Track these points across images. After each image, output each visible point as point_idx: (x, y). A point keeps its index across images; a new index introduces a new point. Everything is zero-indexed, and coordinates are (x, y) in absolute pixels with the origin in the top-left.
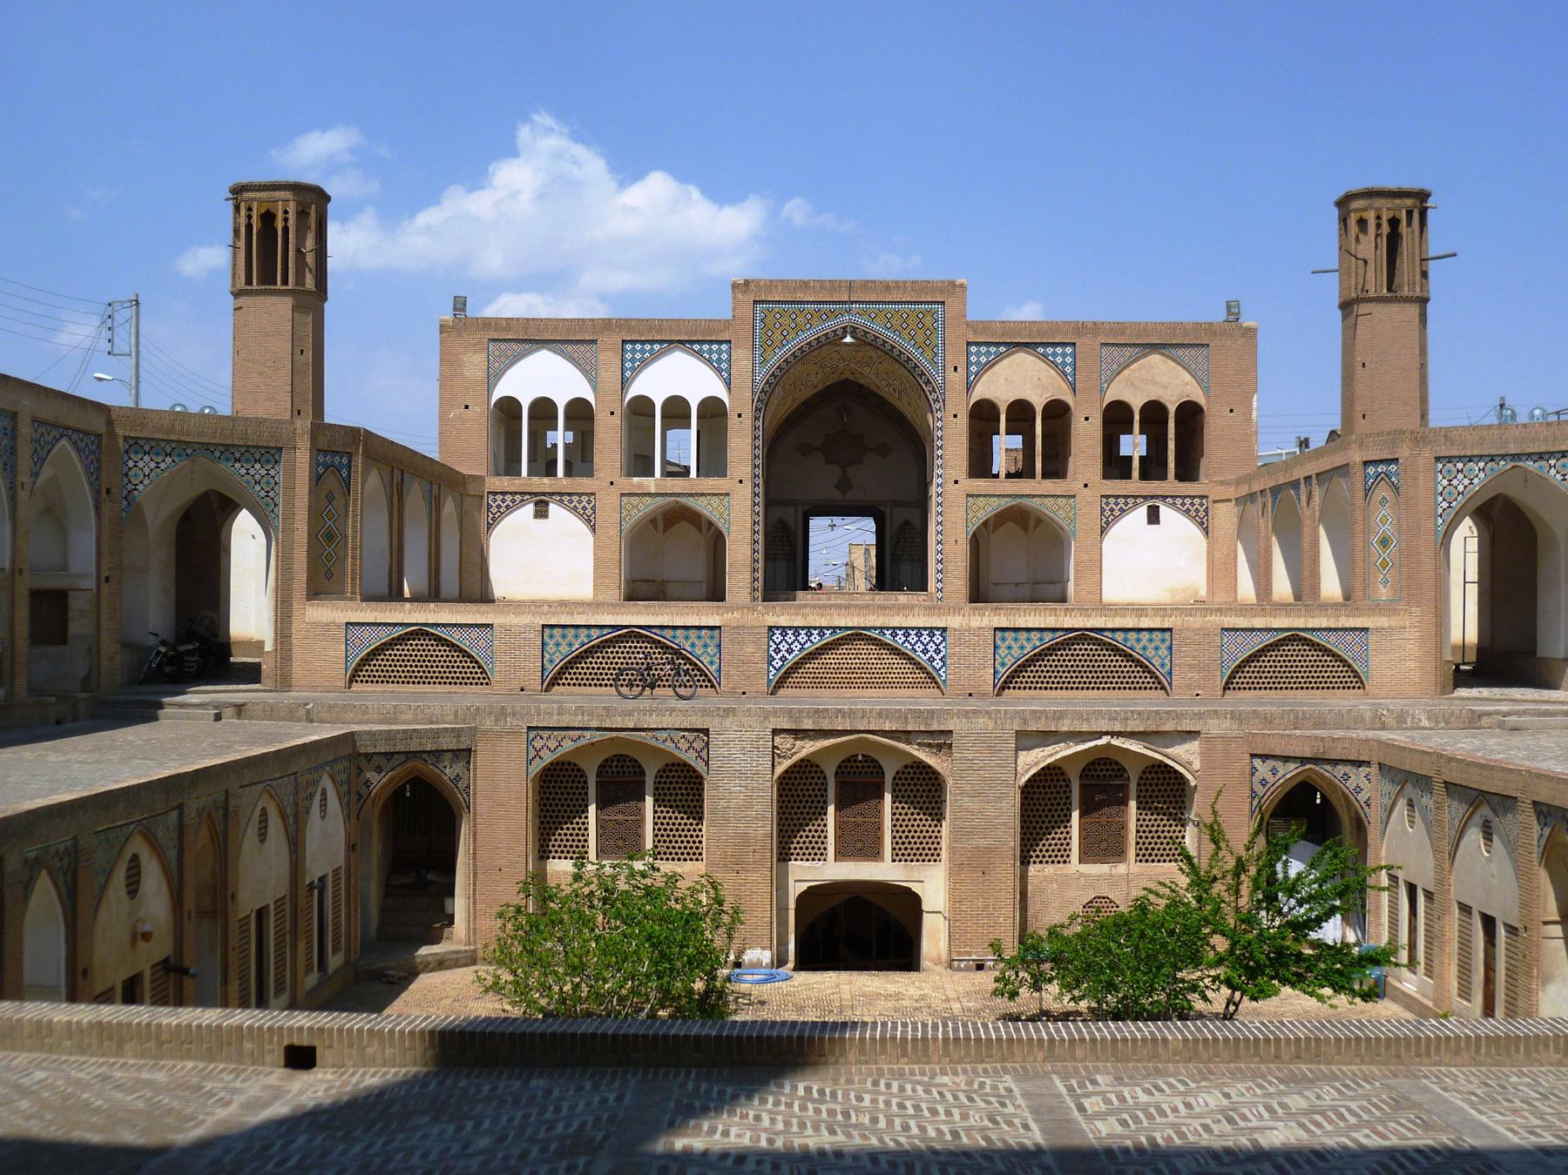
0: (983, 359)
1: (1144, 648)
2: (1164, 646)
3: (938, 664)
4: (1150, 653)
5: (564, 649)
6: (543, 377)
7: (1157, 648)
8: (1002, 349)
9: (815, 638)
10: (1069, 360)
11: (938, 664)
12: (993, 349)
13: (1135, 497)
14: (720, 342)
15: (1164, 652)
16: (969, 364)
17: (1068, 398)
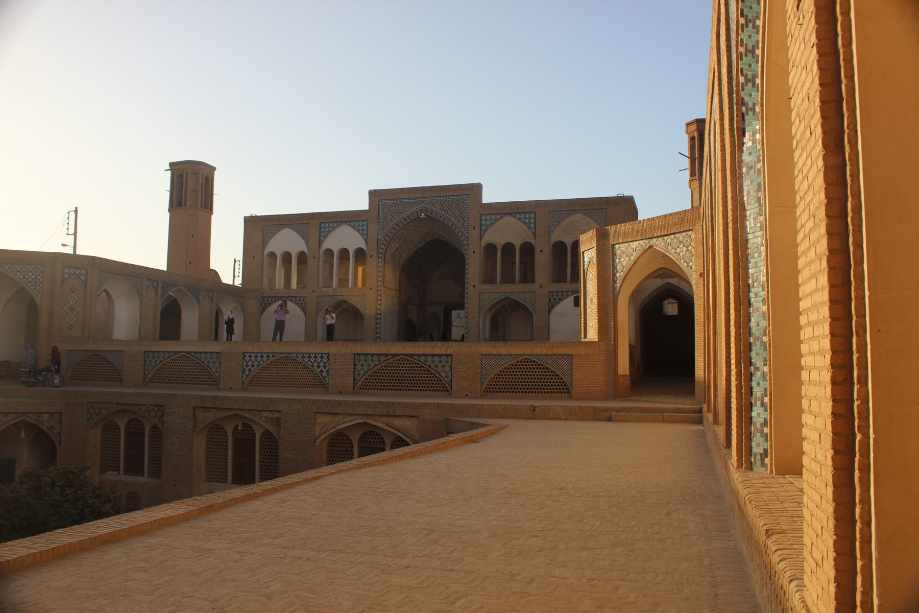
0: (488, 223)
1: (436, 366)
2: (447, 365)
3: (325, 374)
4: (440, 369)
5: (153, 364)
6: (287, 242)
7: (443, 366)
8: (498, 216)
9: (265, 359)
10: (532, 221)
11: (325, 374)
12: (493, 217)
13: (567, 292)
14: (363, 221)
15: (447, 368)
16: (481, 225)
17: (533, 242)
